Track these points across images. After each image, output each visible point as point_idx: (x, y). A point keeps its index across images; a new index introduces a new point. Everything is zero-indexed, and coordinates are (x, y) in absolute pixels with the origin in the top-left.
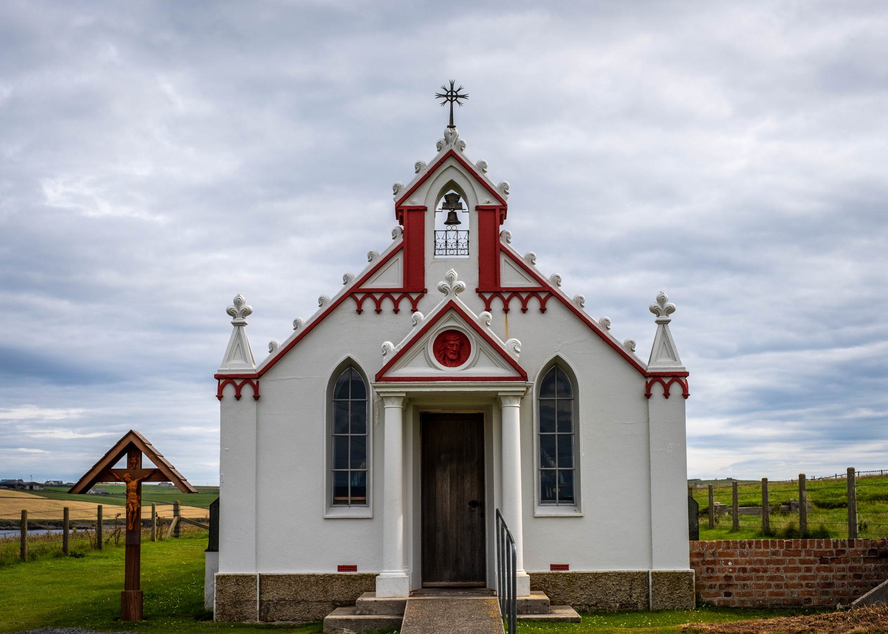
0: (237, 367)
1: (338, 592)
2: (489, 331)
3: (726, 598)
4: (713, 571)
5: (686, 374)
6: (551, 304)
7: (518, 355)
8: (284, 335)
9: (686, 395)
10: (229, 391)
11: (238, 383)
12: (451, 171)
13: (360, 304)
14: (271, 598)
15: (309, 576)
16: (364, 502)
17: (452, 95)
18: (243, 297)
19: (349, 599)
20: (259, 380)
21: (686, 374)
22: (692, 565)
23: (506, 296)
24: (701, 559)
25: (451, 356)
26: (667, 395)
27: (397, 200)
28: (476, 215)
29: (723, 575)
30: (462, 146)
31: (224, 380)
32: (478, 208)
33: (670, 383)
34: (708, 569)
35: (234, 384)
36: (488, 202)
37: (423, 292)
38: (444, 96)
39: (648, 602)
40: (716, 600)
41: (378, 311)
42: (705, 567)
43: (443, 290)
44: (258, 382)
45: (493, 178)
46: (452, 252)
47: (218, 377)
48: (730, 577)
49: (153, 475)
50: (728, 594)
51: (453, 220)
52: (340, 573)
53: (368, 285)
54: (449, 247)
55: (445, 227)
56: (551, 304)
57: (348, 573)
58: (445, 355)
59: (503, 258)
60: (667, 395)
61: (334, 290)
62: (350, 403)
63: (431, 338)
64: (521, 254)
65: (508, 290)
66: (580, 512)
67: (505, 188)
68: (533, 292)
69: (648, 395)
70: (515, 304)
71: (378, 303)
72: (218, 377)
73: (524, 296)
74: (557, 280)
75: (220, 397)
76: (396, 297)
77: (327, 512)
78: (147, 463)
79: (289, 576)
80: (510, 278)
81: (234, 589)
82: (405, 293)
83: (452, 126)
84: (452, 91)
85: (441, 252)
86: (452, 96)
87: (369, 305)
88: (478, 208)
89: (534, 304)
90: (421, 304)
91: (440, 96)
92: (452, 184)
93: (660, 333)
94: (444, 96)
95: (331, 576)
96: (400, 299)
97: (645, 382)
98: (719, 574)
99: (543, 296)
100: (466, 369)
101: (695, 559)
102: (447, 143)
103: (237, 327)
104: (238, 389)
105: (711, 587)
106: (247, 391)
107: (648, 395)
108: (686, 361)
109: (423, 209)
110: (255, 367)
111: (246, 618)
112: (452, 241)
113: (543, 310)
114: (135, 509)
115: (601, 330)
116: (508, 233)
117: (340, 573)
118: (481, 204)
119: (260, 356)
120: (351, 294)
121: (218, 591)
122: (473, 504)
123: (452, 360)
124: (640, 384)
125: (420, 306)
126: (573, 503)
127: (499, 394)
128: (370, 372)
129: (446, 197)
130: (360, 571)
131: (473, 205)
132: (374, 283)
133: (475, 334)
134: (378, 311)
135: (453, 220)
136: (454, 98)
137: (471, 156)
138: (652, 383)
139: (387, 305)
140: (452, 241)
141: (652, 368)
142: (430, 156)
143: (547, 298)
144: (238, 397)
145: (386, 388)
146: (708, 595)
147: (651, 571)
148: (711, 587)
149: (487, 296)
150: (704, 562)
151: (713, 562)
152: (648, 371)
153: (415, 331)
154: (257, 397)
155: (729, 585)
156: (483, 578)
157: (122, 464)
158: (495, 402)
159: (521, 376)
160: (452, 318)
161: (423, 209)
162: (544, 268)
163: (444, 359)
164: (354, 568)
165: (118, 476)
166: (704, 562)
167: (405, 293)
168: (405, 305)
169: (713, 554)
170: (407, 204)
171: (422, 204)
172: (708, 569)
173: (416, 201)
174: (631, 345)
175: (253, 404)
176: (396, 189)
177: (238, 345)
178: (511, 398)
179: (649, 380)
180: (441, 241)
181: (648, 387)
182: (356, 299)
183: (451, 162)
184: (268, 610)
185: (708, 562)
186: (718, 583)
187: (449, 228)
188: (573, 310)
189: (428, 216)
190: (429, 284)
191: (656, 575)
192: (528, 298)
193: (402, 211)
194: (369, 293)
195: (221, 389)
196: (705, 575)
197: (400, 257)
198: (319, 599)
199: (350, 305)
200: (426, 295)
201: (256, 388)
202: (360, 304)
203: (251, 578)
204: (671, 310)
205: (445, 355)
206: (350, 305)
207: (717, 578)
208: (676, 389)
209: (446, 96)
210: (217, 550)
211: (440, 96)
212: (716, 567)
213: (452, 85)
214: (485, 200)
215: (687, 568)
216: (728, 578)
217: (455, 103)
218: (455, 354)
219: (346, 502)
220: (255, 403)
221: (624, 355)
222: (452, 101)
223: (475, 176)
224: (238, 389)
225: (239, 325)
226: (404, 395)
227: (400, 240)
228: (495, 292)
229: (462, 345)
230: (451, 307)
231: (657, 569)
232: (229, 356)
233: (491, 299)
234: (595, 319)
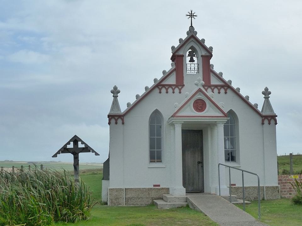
0: (115, 113)
1: (154, 194)
2: (212, 99)
3: (290, 195)
4: (285, 186)
5: (277, 116)
7: (223, 108)
8: (133, 100)
9: (276, 124)
10: (113, 121)
11: (116, 118)
12: (192, 42)
13: (160, 90)
14: (129, 197)
15: (143, 189)
16: (161, 161)
17: (192, 15)
18: (117, 86)
19: (157, 197)
20: (124, 117)
21: (277, 116)
22: (279, 184)
23: (213, 88)
24: (281, 182)
25: (200, 108)
26: (269, 124)
27: (173, 52)
28: (201, 58)
29: (289, 187)
30: (196, 33)
32: (202, 56)
33: (270, 120)
34: (283, 185)
36: (206, 54)
37: (183, 86)
38: (189, 15)
39: (264, 197)
40: (286, 196)
41: (167, 92)
43: (196, 85)
45: (207, 44)
46: (193, 71)
48: (291, 188)
50: (290, 194)
51: (192, 60)
52: (154, 187)
53: (164, 83)
54: (191, 70)
55: (190, 63)
56: (229, 91)
57: (157, 187)
58: (197, 108)
59: (211, 74)
60: (269, 124)
61: (151, 84)
62: (156, 126)
63: (192, 101)
65: (213, 86)
66: (240, 165)
67: (211, 48)
68: (222, 86)
69: (263, 124)
70: (216, 90)
71: (167, 90)
72: (109, 116)
73: (219, 88)
74: (230, 82)
75: (109, 123)
79: (136, 189)
80: (214, 81)
81: (116, 193)
82: (176, 86)
83: (192, 26)
84: (191, 14)
85: (189, 71)
86: (192, 16)
87: (164, 90)
88: (202, 56)
89: (222, 91)
91: (188, 15)
92: (192, 48)
93: (266, 102)
94: (189, 15)
95: (151, 189)
97: (262, 120)
98: (287, 187)
99: (226, 88)
100: (205, 113)
101: (279, 182)
102: (191, 32)
103: (115, 98)
105: (285, 192)
106: (120, 121)
107: (263, 124)
108: (276, 112)
109: (183, 56)
111: (120, 204)
112: (193, 68)
113: (226, 93)
115: (246, 100)
116: (213, 65)
117: (154, 187)
118: (203, 54)
119: (123, 108)
121: (110, 194)
122: (199, 163)
123: (200, 110)
124: (260, 120)
125: (182, 91)
126: (236, 162)
127: (217, 122)
128: (166, 114)
129: (189, 52)
130: (161, 187)
131: (200, 54)
132: (166, 82)
133: (209, 101)
134: (167, 92)
135: (192, 60)
136: (192, 16)
137: (200, 36)
138: (264, 119)
139: (170, 90)
140: (193, 68)
141: (264, 114)
142: (184, 36)
143: (227, 89)
146: (284, 194)
147: (265, 186)
148: (285, 192)
149: (206, 88)
151: (285, 183)
152: (263, 115)
153: (186, 99)
154: (123, 123)
158: (212, 125)
159: (224, 116)
160: (200, 95)
161: (183, 56)
162: (226, 78)
163: (197, 109)
164: (159, 186)
166: (282, 183)
168: (177, 90)
169: (285, 180)
170: (177, 54)
171: (182, 54)
172: (283, 185)
173: (181, 53)
174: (256, 105)
176: (173, 48)
177: (115, 103)
178: (221, 124)
179: (263, 118)
180: (188, 68)
182: (159, 88)
183: (192, 39)
184: (128, 201)
185: (283, 183)
186: (287, 190)
187: (192, 63)
188: (236, 92)
189: (184, 58)
190: (185, 82)
191: (267, 187)
192: (221, 88)
193: (175, 56)
194: (164, 86)
195: (110, 120)
196: (282, 187)
197: (174, 73)
198: (147, 197)
200: (184, 87)
201: (123, 120)
203: (121, 190)
204: (270, 93)
205: (197, 108)
206: (157, 90)
207: (287, 189)
208: (272, 122)
209: (190, 15)
210: (108, 179)
211: (188, 15)
212: (286, 184)
213: (191, 12)
214: (204, 53)
215: (277, 185)
217: (193, 18)
218: (200, 107)
219: (155, 162)
220: (123, 125)
221: (253, 108)
222: (191, 17)
223: (201, 43)
225: (115, 97)
226: (183, 122)
227: (174, 67)
228: (209, 86)
229: (203, 104)
230: (200, 90)
231: (267, 185)
232: (112, 109)
233: (207, 88)
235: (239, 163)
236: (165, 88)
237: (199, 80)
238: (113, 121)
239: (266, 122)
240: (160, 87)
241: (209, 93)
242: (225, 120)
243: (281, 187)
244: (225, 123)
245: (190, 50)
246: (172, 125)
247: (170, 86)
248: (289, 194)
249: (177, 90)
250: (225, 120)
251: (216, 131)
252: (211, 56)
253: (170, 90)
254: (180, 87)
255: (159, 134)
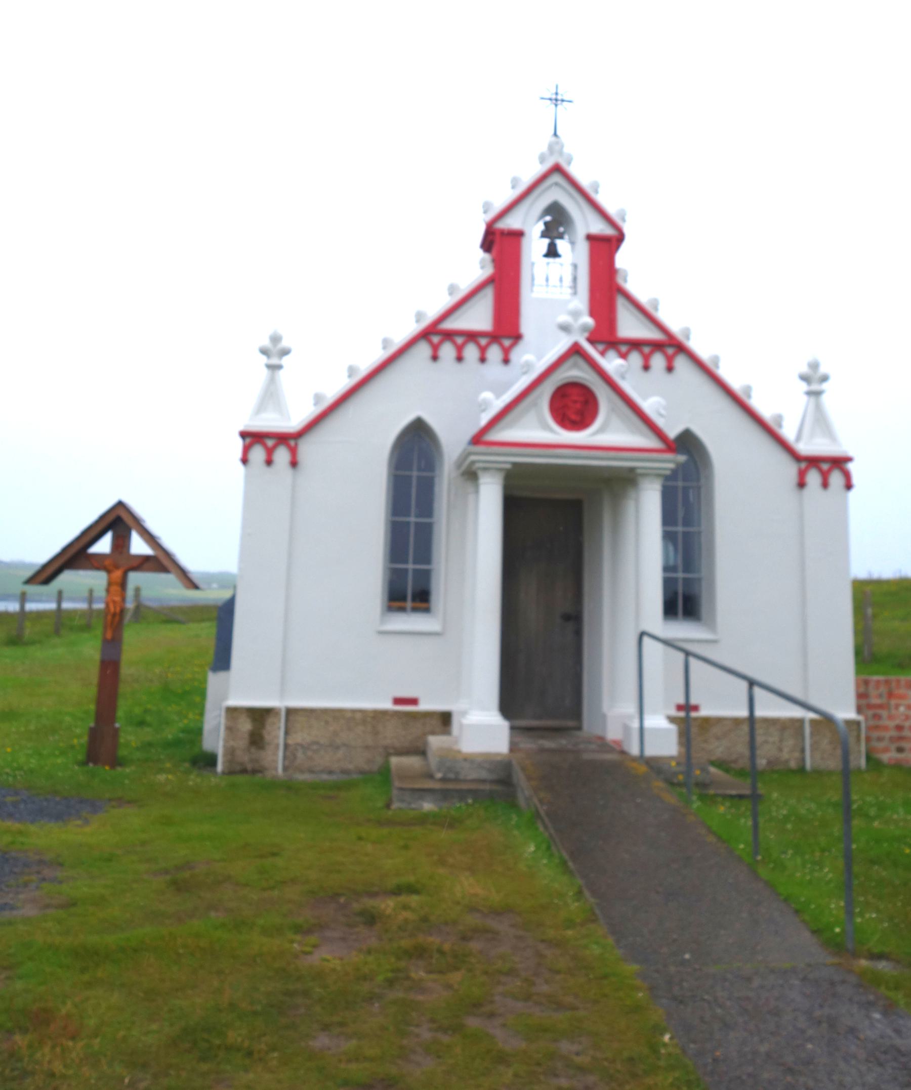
6: (681, 362)
10: (258, 454)
13: (435, 348)
16: (427, 610)
31: (252, 438)
35: (265, 445)
37: (517, 337)
41: (460, 359)
42: (870, 713)
44: (296, 445)
47: (244, 435)
49: (143, 563)
50: (900, 750)
56: (681, 362)
64: (643, 298)
68: (657, 346)
69: (801, 484)
71: (460, 349)
72: (244, 435)
73: (647, 350)
75: (245, 461)
76: (483, 341)
77: (382, 622)
78: (138, 546)
82: (494, 337)
90: (514, 355)
96: (488, 345)
104: (270, 452)
106: (282, 455)
107: (801, 484)
110: (293, 422)
113: (670, 369)
114: (118, 610)
120: (425, 334)
124: (791, 469)
134: (460, 359)
139: (471, 351)
144: (269, 462)
145: (480, 456)
148: (880, 739)
150: (870, 706)
151: (881, 706)
154: (294, 464)
155: (901, 738)
156: (576, 712)
157: (103, 546)
165: (97, 562)
166: (870, 706)
167: (494, 337)
168: (494, 353)
175: (288, 471)
179: (803, 465)
181: (802, 475)
182: (431, 342)
192: (652, 353)
194: (449, 335)
195: (246, 450)
196: (872, 723)
199: (423, 350)
201: (293, 451)
202: (435, 348)
207: (886, 728)
212: (884, 713)
216: (899, 728)
224: (270, 452)
234: (735, 384)
235: (712, 625)
236: (454, 343)
237: (576, 314)
238: (258, 454)
239: (813, 478)
240: (436, 339)
241: (612, 363)
242: (669, 462)
243: (866, 719)
244: (667, 478)
245: (548, 218)
246: (471, 475)
247: (472, 336)
248: (893, 747)
249: (494, 353)
250: (669, 462)
251: (630, 506)
252: (620, 238)
253: (471, 351)
254: (507, 343)
255: (427, 506)
